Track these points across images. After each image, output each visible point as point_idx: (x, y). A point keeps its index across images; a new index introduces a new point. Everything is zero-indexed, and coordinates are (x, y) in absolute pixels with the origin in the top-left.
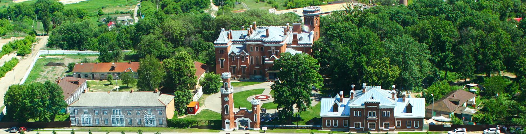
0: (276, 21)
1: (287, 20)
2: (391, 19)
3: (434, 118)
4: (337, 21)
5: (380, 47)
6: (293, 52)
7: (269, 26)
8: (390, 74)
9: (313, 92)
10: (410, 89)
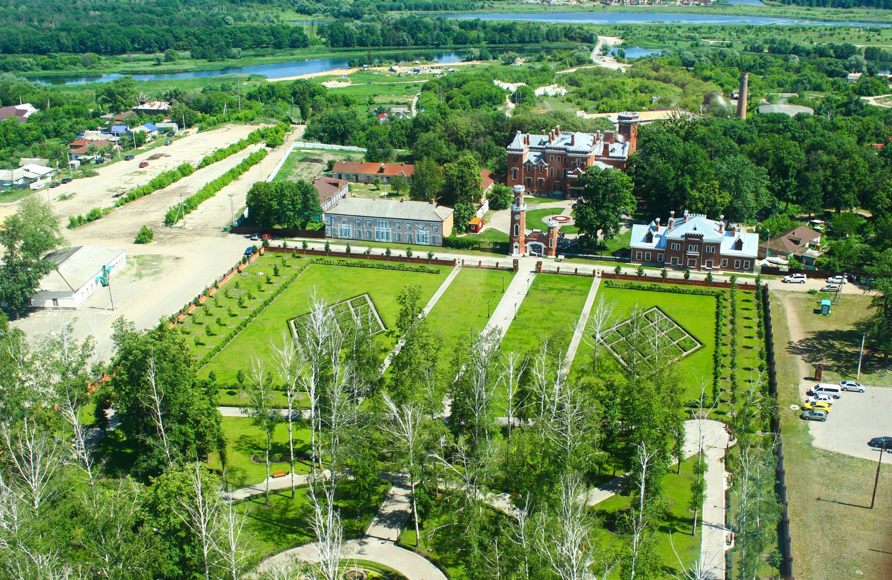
0: (584, 126)
1: (598, 126)
2: (725, 134)
3: (768, 258)
4: (659, 132)
5: (709, 168)
6: (603, 166)
7: (576, 132)
8: (719, 200)
9: (623, 216)
10: (742, 222)
